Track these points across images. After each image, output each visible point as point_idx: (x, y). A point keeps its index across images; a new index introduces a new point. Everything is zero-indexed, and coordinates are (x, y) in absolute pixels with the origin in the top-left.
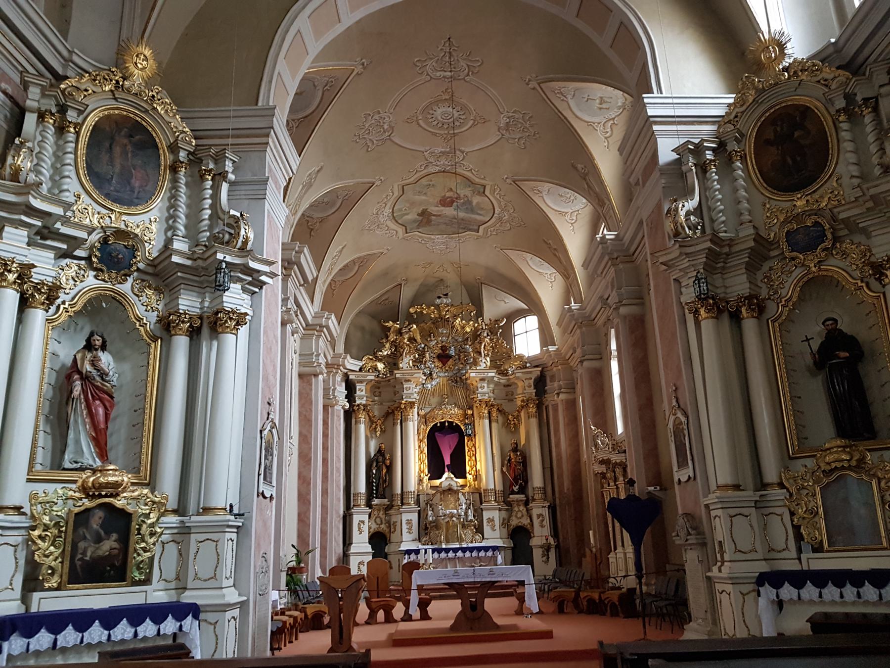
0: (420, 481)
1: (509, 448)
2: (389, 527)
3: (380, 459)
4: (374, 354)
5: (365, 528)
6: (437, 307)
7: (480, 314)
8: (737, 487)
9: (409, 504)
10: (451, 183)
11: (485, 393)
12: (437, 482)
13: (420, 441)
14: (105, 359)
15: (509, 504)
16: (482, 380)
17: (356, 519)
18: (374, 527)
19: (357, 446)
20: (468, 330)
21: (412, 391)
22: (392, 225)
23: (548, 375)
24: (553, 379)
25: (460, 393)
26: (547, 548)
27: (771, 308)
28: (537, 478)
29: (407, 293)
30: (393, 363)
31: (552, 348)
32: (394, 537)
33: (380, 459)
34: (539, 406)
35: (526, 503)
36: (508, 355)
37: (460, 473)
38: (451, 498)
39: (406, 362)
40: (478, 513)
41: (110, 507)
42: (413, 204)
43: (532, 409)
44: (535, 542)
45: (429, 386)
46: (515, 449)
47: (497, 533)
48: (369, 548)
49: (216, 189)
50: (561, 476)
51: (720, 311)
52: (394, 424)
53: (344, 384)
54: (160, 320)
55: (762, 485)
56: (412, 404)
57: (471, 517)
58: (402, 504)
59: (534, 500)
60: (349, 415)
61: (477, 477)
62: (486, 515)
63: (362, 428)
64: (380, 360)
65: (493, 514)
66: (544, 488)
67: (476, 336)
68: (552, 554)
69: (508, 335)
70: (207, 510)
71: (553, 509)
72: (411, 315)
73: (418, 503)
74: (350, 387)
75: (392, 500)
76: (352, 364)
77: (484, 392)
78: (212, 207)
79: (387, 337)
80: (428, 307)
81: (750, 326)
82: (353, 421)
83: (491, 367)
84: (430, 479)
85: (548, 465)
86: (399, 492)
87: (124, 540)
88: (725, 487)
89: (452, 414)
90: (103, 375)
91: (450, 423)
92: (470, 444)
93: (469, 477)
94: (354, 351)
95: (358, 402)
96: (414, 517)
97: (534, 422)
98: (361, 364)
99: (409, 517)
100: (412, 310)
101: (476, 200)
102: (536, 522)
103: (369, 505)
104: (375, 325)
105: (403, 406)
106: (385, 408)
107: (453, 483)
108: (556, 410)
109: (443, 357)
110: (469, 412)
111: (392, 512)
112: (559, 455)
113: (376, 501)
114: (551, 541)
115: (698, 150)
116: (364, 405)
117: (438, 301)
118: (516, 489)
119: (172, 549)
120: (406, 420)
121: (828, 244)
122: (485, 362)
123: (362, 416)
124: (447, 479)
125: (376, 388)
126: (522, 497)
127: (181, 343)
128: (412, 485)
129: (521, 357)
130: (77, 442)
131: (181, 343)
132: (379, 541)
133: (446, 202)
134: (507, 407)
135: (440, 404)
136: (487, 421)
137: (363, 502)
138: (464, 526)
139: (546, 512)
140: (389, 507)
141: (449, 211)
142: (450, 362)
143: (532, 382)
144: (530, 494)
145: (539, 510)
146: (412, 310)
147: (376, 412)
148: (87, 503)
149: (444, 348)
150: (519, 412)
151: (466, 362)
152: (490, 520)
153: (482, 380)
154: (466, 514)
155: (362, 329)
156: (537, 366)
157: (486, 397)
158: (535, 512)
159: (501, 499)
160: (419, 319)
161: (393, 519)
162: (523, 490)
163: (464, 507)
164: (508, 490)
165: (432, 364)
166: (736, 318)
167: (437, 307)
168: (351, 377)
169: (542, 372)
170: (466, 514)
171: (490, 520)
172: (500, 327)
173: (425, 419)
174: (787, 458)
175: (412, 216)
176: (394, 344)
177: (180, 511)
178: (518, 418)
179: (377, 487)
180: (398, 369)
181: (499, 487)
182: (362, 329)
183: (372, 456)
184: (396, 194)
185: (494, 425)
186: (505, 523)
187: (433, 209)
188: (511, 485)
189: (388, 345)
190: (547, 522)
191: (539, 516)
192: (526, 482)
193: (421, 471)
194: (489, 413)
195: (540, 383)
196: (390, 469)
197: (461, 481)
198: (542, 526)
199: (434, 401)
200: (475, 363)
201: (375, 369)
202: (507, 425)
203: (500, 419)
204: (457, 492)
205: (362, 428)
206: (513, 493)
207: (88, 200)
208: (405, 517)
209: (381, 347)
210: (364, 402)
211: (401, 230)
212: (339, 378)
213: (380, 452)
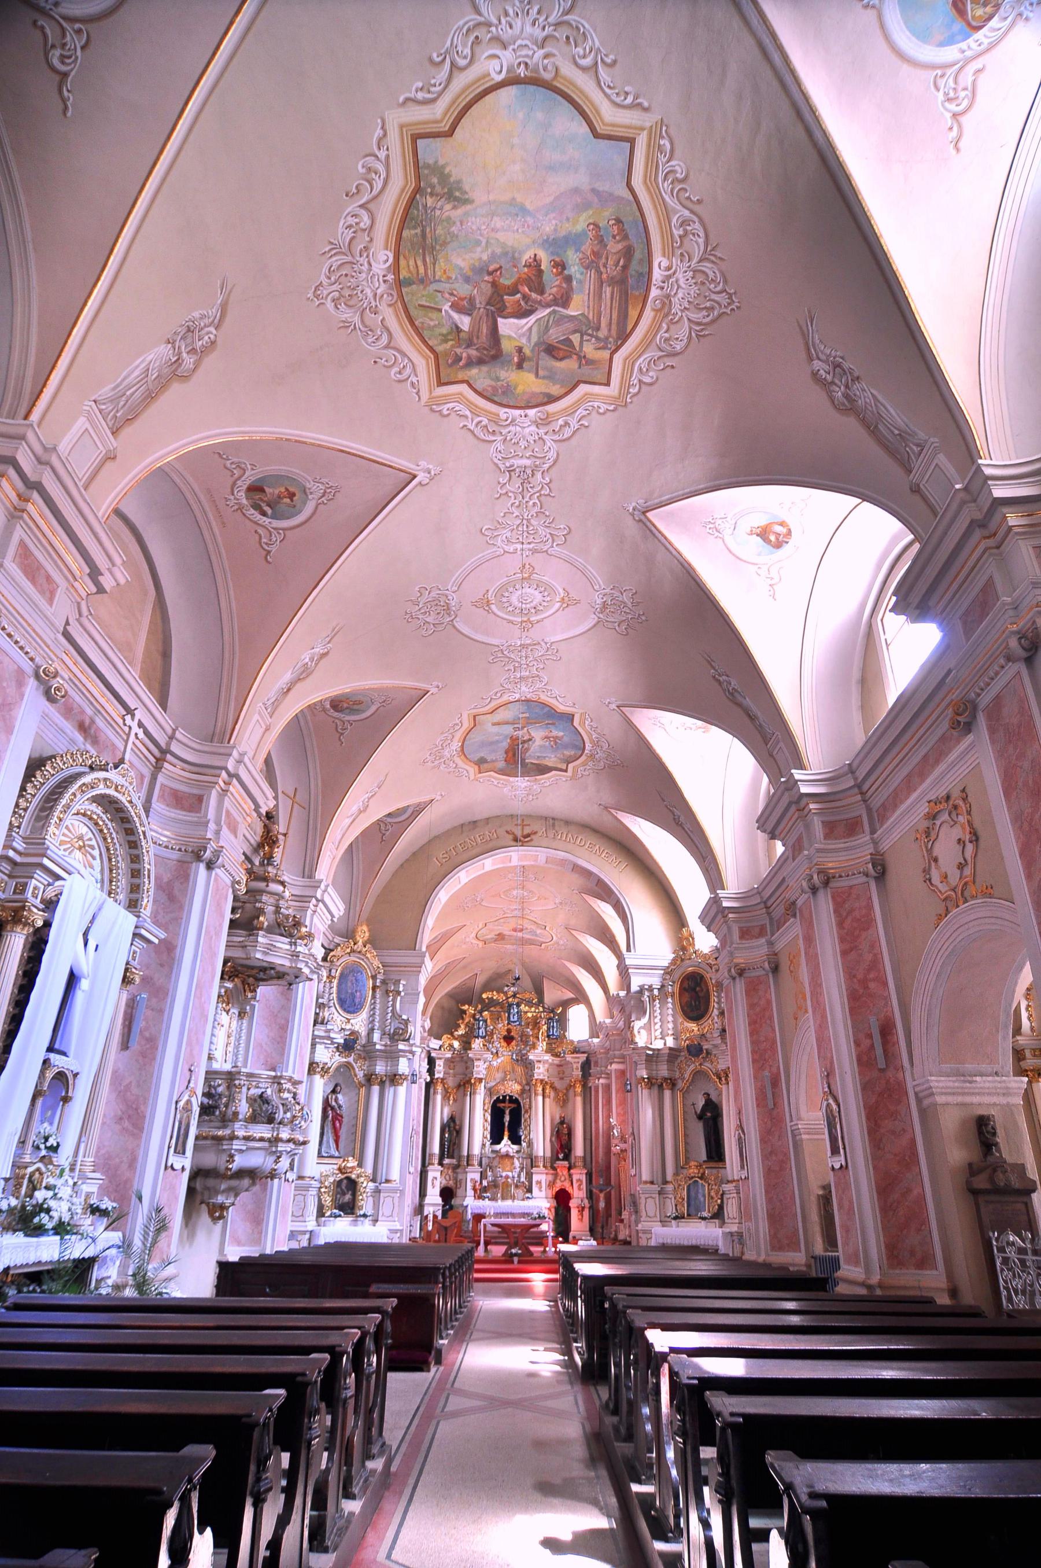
0: (484, 1145)
1: (557, 1120)
2: (456, 1183)
3: (452, 1125)
4: (452, 1034)
5: (437, 1184)
6: (505, 993)
7: (541, 1001)
8: (652, 1183)
9: (473, 1165)
10: (520, 922)
11: (539, 1074)
12: (497, 1147)
13: (485, 1111)
14: (340, 1096)
15: (554, 1168)
16: (539, 1061)
17: (431, 1175)
18: (444, 1182)
19: (434, 1113)
20: (530, 1015)
21: (480, 1069)
22: (475, 942)
23: (593, 1060)
24: (596, 1064)
25: (519, 1069)
26: (582, 1210)
27: (680, 1084)
28: (579, 1149)
29: (481, 980)
30: (467, 1045)
31: (596, 1040)
32: (459, 1192)
33: (452, 1125)
34: (585, 1086)
35: (569, 1168)
36: (562, 1038)
37: (516, 1140)
38: (507, 1161)
39: (477, 1044)
40: (529, 1176)
41: (348, 1179)
42: (492, 931)
43: (579, 1089)
44: (573, 1204)
45: (495, 1063)
46: (562, 1122)
47: (543, 1194)
48: (439, 1200)
49: (394, 1001)
50: (597, 1148)
51: (652, 1084)
52: (465, 1095)
53: (426, 1060)
54: (365, 1075)
55: (665, 1182)
56: (480, 1080)
57: (523, 1179)
58: (468, 1165)
59: (575, 1167)
60: (428, 1086)
61: (530, 1144)
62: (535, 1178)
63: (439, 1098)
64: (456, 1039)
65: (541, 1176)
66: (584, 1157)
67: (535, 1023)
68: (586, 1213)
69: (562, 1021)
70: (387, 1181)
71: (589, 1175)
72: (483, 1000)
73: (480, 1165)
74: (431, 1062)
75: (459, 1161)
76: (435, 1044)
77: (540, 1072)
78: (392, 1011)
79: (463, 1019)
80: (498, 992)
81: (667, 1094)
82: (432, 1091)
83: (546, 1052)
84: (492, 1144)
85: (588, 1137)
86: (465, 1153)
87: (354, 1195)
88: (646, 1182)
89: (513, 1088)
90: (340, 1107)
91: (511, 1097)
92: (527, 1116)
93: (524, 1144)
94: (435, 1029)
95: (437, 1076)
96: (477, 1177)
97: (579, 1100)
98: (440, 1043)
99: (473, 1175)
100: (484, 996)
101: (539, 931)
102: (575, 1185)
103: (441, 1164)
104: (453, 1003)
105: (473, 1081)
106: (457, 1080)
107: (510, 1150)
108: (597, 1091)
109: (508, 1039)
110: (527, 1088)
111: (459, 1170)
112: (597, 1129)
113: (446, 1161)
114: (586, 1201)
115: (651, 989)
116: (442, 1079)
117: (506, 989)
118: (561, 1156)
119: (371, 1199)
120: (475, 1093)
121: (704, 1055)
122: (542, 1046)
123: (440, 1088)
124: (506, 1145)
125: (449, 1062)
126: (566, 1163)
127: (376, 1089)
128: (476, 1150)
129: (572, 1042)
130: (328, 1142)
131: (376, 1089)
132: (447, 1194)
133: (515, 930)
134: (558, 1084)
135: (504, 1079)
136: (540, 1098)
137: (436, 1161)
138: (517, 1186)
139: (584, 1178)
140: (458, 1166)
141: (520, 934)
142: (514, 1043)
143: (579, 1065)
144: (573, 1161)
145: (579, 1175)
146: (484, 996)
147: (451, 1082)
148: (340, 1176)
149: (509, 1031)
150: (567, 1090)
151: (526, 1043)
152: (539, 1183)
153: (539, 1061)
154: (519, 1176)
155: (443, 1008)
156: (584, 1053)
157: (541, 1077)
158: (575, 1178)
159: (549, 1165)
160: (489, 1004)
161: (460, 1177)
162: (567, 1157)
163: (518, 1170)
164: (555, 1158)
165: (498, 1044)
166: (661, 1086)
167: (505, 993)
168: (433, 1055)
169: (587, 1058)
170: (519, 1176)
171: (539, 1183)
172: (558, 1015)
173: (490, 1091)
174: (678, 1169)
175: (492, 936)
176: (467, 1025)
177: (374, 1180)
178: (566, 1094)
179: (448, 1148)
180: (470, 1049)
181: (548, 1154)
182: (443, 1008)
183: (445, 1121)
184: (481, 926)
185: (547, 1100)
186: (551, 1185)
187: (507, 933)
188: (558, 1153)
189: (462, 1026)
190: (584, 1186)
191: (579, 1180)
192: (570, 1151)
193: (484, 1137)
194: (543, 1090)
195: (586, 1066)
196: (459, 1132)
197: (515, 1147)
198: (579, 1189)
199: (499, 1076)
200: (534, 1046)
201: (451, 1046)
202: (557, 1100)
203: (552, 1094)
204: (512, 1157)
205: (439, 1098)
206: (558, 1159)
207: (336, 1013)
208: (470, 1176)
209: (457, 1027)
210: (441, 1075)
211: (481, 944)
212: (423, 1055)
213: (452, 1119)
